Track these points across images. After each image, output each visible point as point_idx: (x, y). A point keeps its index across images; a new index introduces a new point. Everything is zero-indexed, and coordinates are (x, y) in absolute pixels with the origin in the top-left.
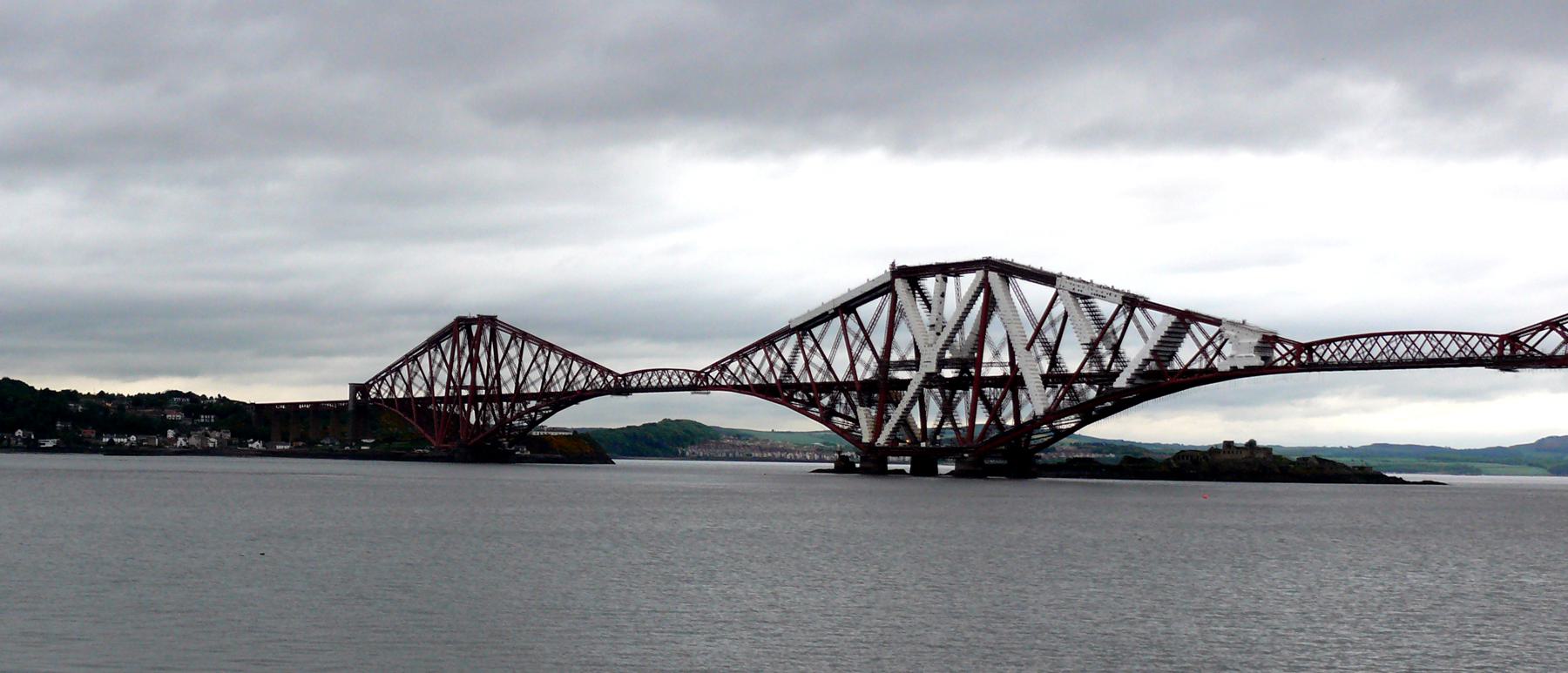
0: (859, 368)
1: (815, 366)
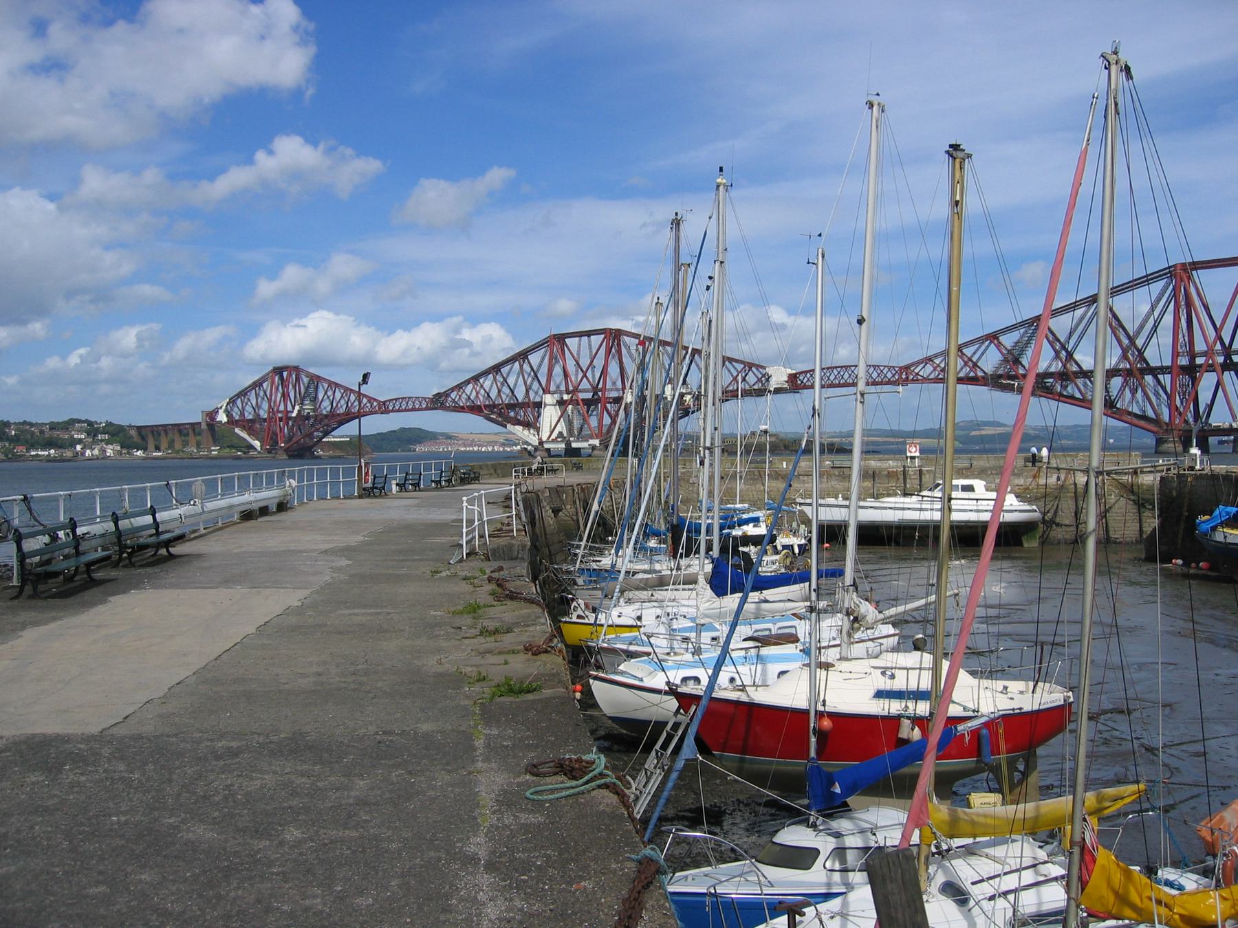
0: (532, 394)
1: (504, 393)
